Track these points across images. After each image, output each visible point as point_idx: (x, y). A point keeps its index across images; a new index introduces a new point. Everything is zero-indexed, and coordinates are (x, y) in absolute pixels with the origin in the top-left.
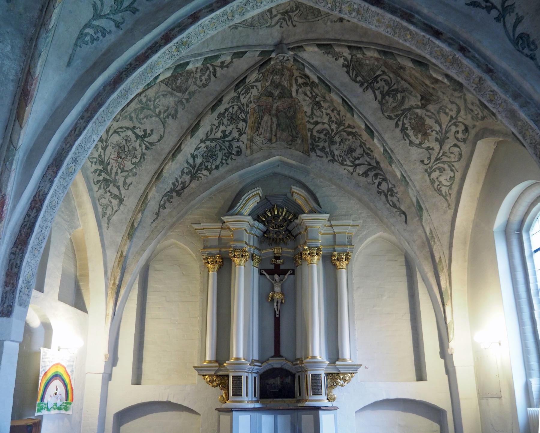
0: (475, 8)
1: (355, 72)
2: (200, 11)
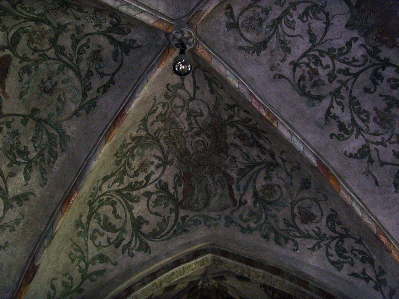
0: (356, 278)
1: (271, 290)
2: (134, 284)
